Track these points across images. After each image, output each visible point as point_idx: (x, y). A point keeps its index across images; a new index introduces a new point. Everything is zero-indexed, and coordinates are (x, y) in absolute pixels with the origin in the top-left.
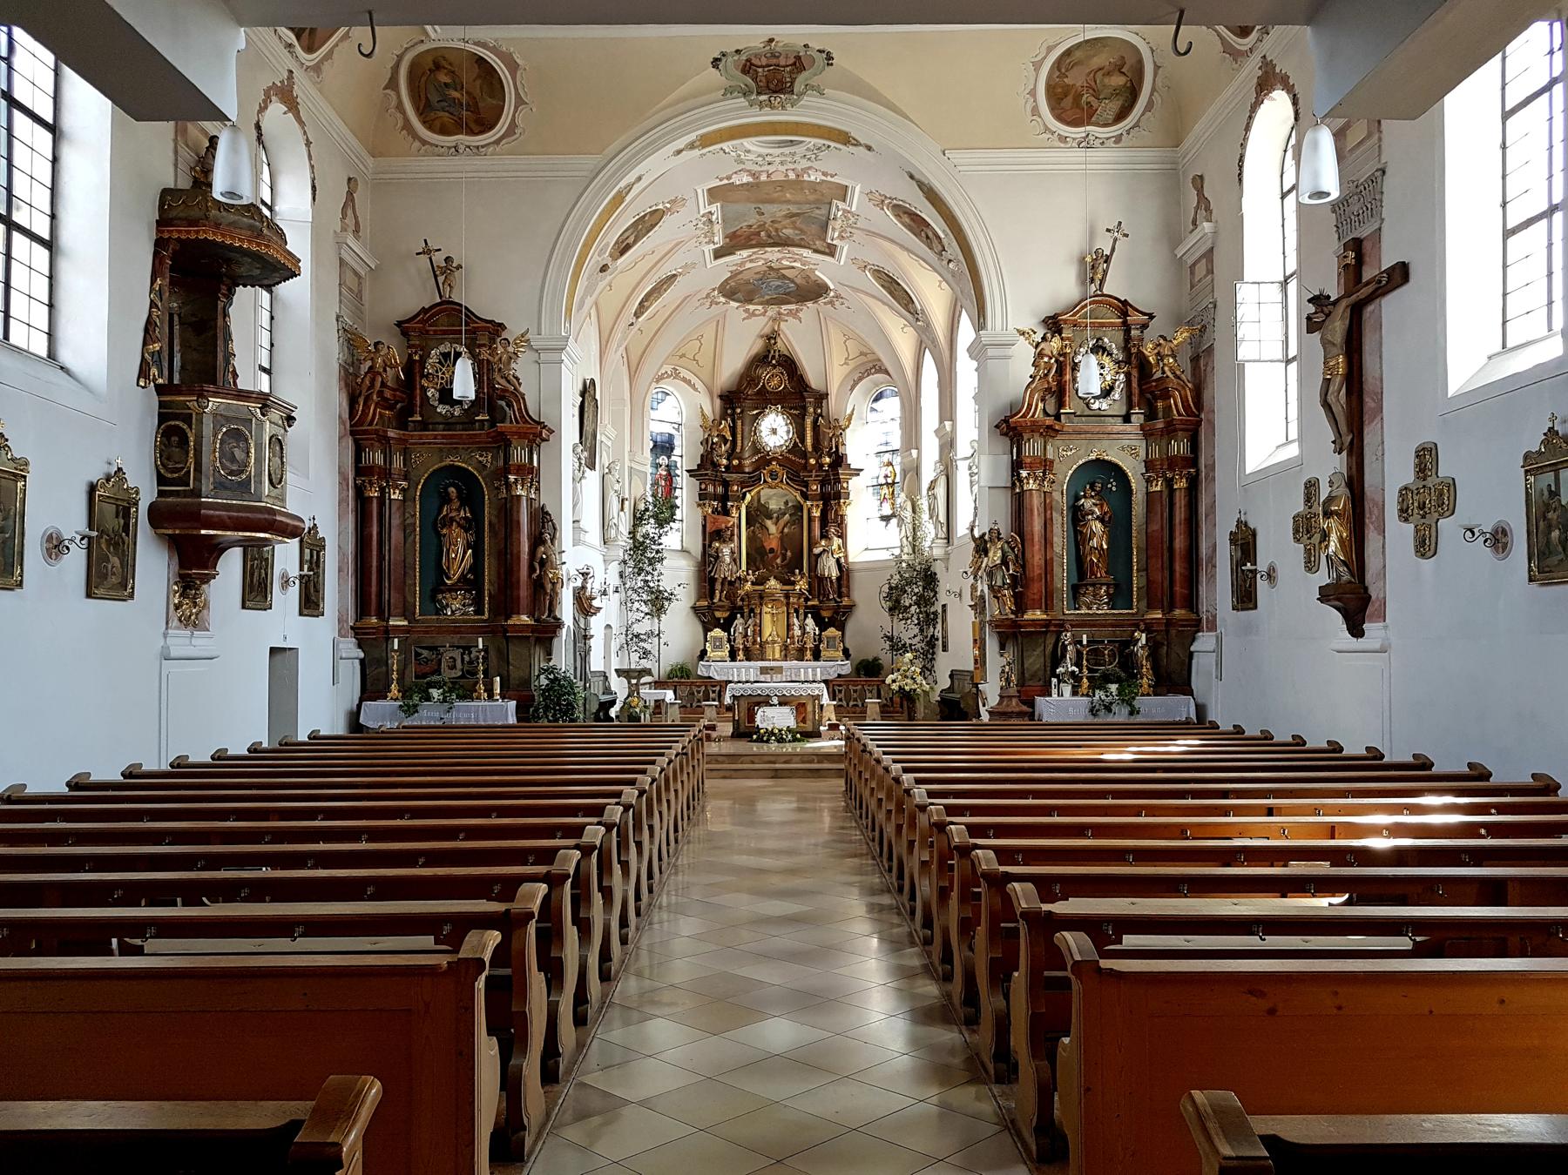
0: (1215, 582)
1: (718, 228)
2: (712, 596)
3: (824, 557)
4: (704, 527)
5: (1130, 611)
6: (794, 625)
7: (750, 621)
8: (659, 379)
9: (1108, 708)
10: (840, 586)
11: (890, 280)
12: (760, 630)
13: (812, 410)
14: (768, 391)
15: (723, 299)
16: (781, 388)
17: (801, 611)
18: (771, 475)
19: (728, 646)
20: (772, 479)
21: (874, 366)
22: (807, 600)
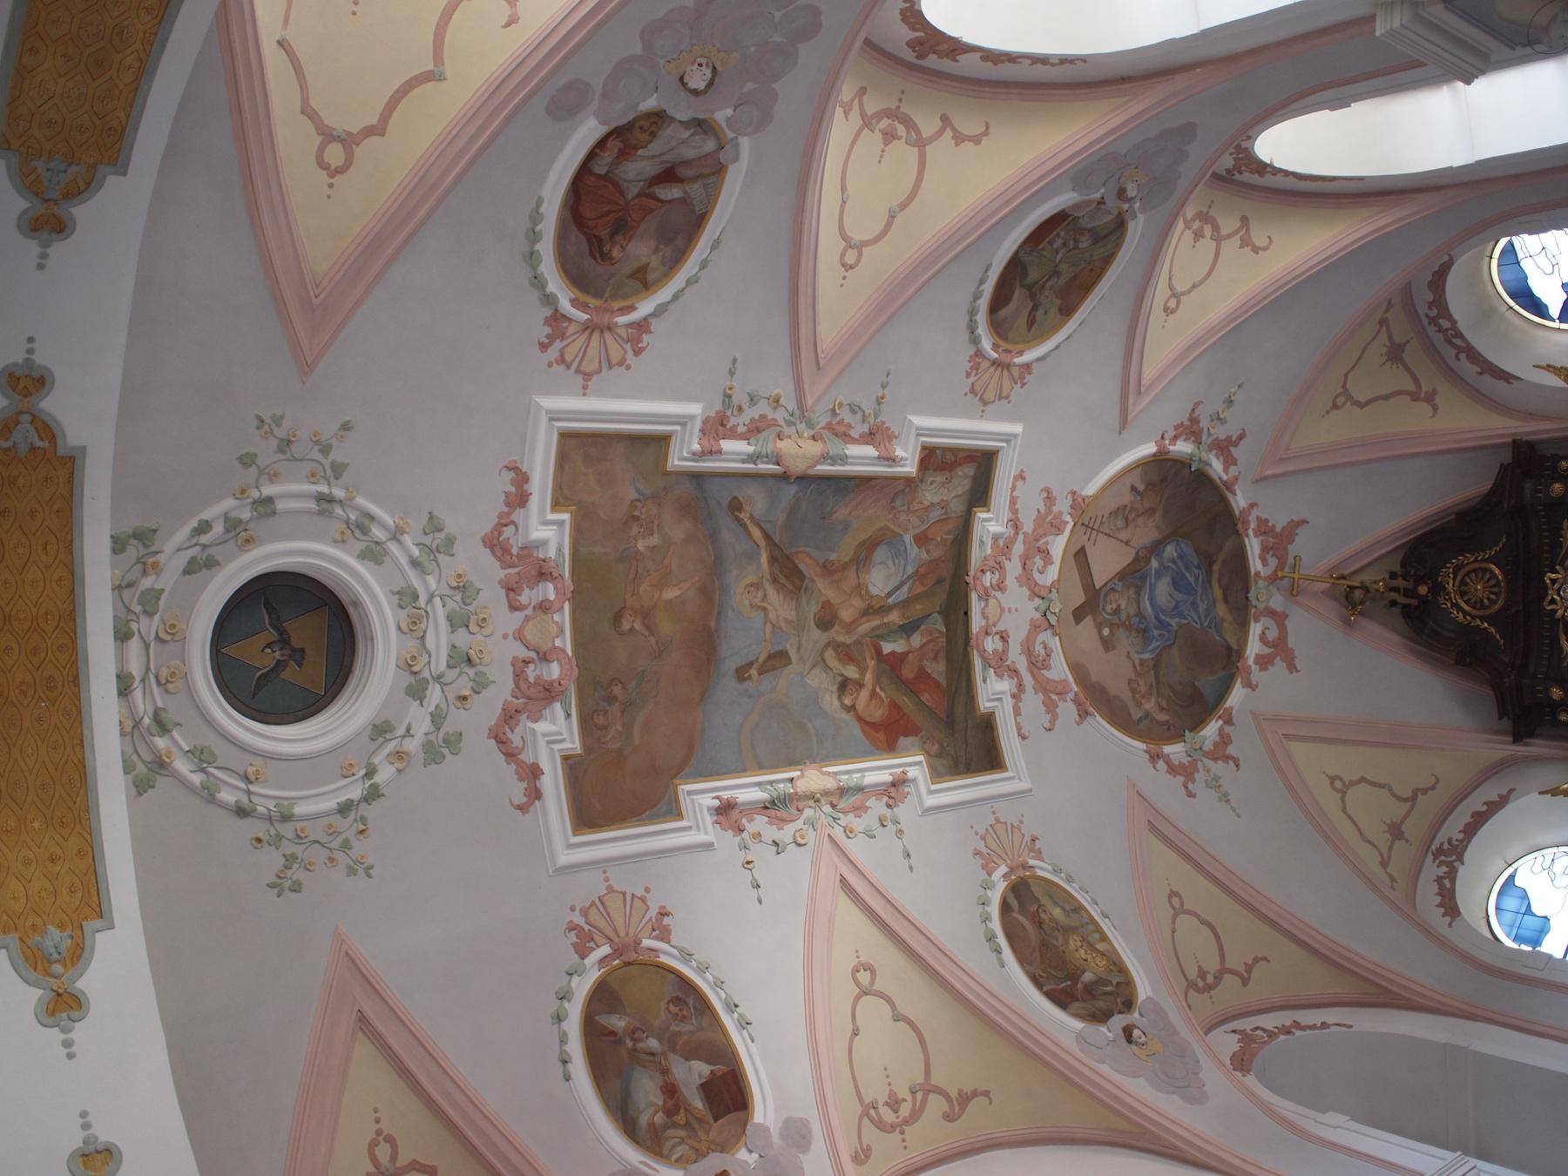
1: (813, 779)
8: (1450, 907)
11: (1018, 294)
15: (1211, 730)
21: (1433, 320)
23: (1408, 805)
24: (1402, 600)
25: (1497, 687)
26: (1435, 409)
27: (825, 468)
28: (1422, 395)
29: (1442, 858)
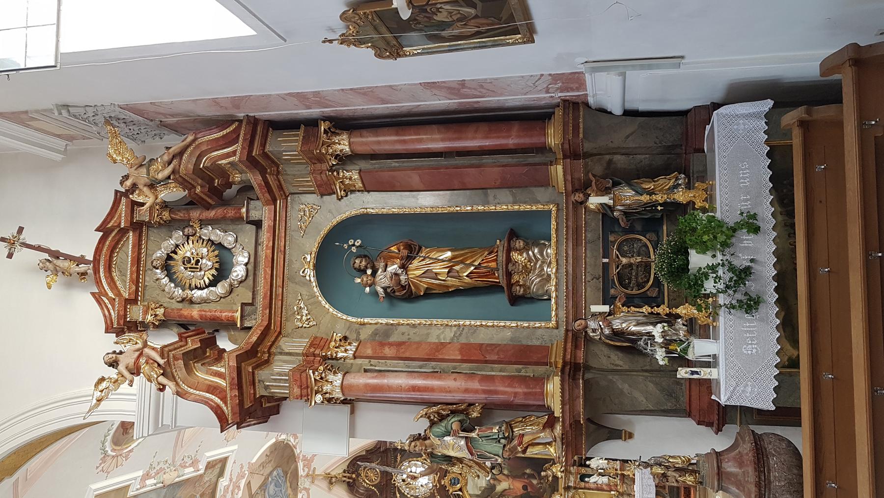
0: (491, 82)
5: (554, 213)
9: (742, 275)
14: (380, 482)
18: (454, 484)
20: (458, 484)
24: (348, 480)
27: (177, 480)
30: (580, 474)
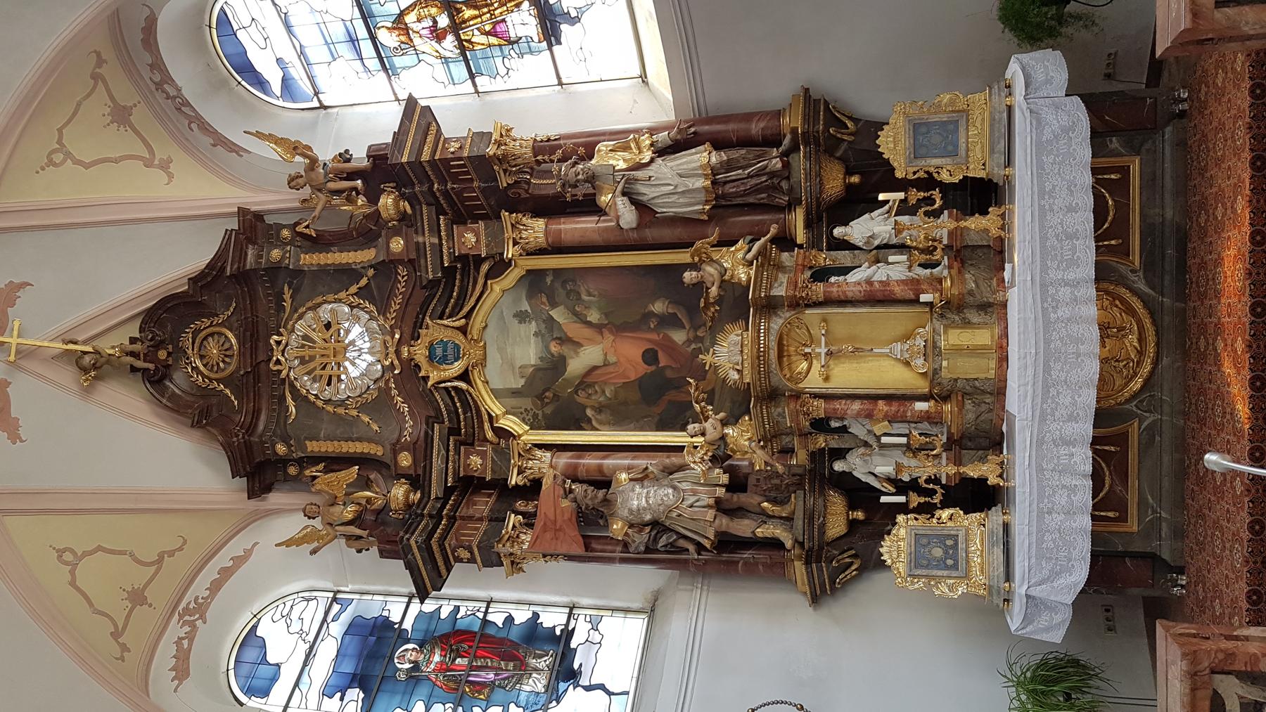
2: (776, 544)
3: (647, 193)
4: (570, 558)
6: (869, 282)
7: (857, 429)
10: (746, 142)
12: (889, 398)
13: (276, 254)
14: (238, 369)
16: (230, 335)
17: (823, 258)
18: (444, 360)
19: (945, 514)
20: (456, 360)
21: (159, 86)
22: (785, 241)
23: (153, 568)
25: (228, 448)
26: (171, 176)
28: (156, 162)
29: (187, 618)
30: (811, 268)
